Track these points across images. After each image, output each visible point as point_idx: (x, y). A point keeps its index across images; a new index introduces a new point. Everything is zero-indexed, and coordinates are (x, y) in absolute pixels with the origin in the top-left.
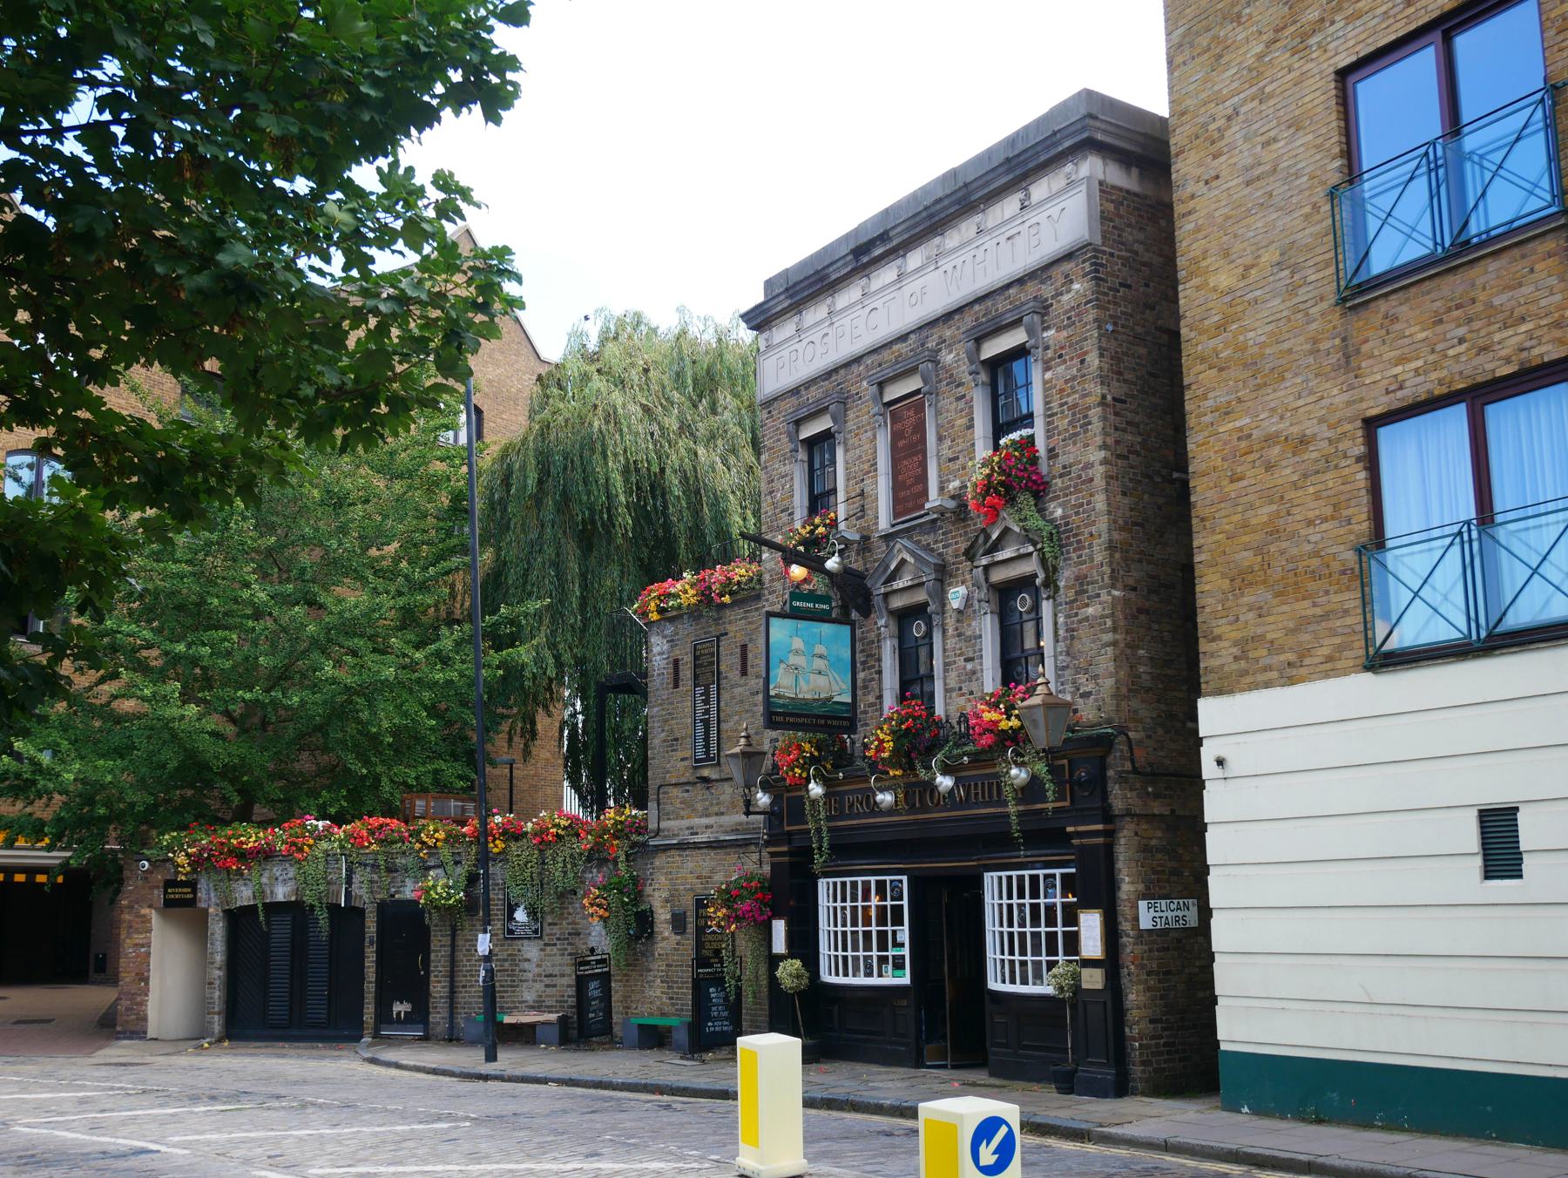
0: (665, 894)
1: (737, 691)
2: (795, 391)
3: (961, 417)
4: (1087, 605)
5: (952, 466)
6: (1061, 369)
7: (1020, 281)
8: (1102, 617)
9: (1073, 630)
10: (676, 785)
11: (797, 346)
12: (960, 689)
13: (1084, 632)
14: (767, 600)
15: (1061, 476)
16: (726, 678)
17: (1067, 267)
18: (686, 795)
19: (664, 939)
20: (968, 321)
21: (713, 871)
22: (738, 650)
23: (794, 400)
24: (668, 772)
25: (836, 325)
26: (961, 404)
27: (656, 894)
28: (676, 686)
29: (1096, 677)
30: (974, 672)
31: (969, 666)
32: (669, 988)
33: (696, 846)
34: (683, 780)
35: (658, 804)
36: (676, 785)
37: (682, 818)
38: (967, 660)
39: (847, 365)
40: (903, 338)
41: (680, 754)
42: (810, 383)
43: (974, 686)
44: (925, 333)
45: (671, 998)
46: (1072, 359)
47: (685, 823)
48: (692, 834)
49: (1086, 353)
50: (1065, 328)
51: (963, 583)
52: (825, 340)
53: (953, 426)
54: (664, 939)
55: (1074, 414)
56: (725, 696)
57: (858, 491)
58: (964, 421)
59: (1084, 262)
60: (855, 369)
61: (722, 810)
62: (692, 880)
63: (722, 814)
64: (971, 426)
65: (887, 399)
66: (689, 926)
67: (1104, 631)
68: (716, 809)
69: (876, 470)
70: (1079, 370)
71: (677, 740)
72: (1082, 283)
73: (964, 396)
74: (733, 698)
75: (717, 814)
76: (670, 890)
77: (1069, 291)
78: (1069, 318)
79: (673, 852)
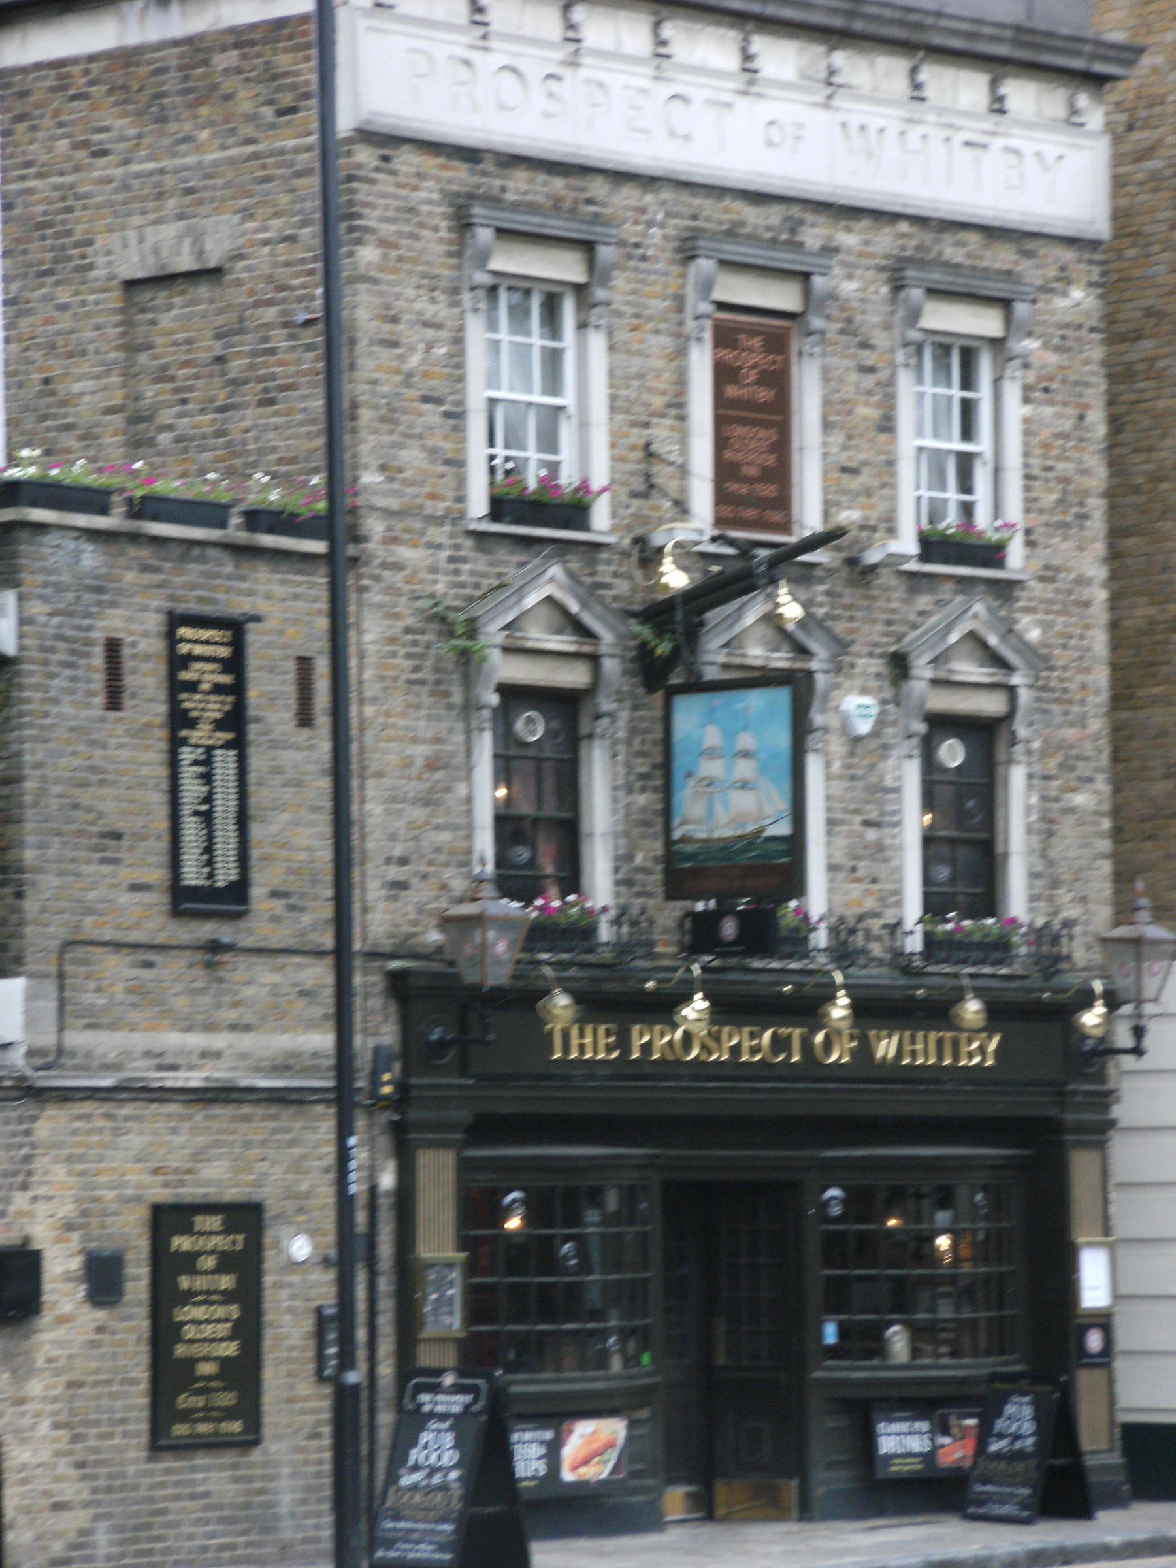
0: (67, 1209)
1: (289, 757)
2: (470, 155)
3: (867, 404)
4: (1074, 790)
5: (853, 483)
6: (1048, 411)
7: (994, 233)
8: (1096, 813)
9: (1052, 821)
10: (117, 946)
11: (476, 57)
12: (854, 869)
13: (1067, 827)
14: (377, 578)
15: (1042, 579)
16: (258, 720)
17: (1068, 255)
18: (147, 974)
19: (62, 1320)
20: (885, 241)
21: (199, 1156)
22: (291, 665)
23: (460, 175)
24: (89, 911)
25: (584, 73)
26: (869, 381)
27: (42, 1209)
28: (114, 699)
29: (1083, 900)
30: (879, 847)
31: (871, 835)
32: (75, 1439)
33: (162, 1095)
34: (135, 936)
35: (62, 988)
36: (117, 946)
37: (133, 1028)
38: (868, 823)
39: (621, 177)
40: (759, 198)
41: (127, 875)
42: (513, 161)
43: (881, 870)
44: (795, 211)
45: (81, 1465)
46: (1065, 404)
47: (139, 1040)
48: (160, 1068)
49: (1087, 407)
50: (1058, 349)
51: (864, 691)
52: (553, 85)
53: (849, 412)
54: (62, 1320)
55: (1064, 492)
56: (257, 761)
57: (642, 441)
58: (874, 413)
59: (1091, 262)
60: (627, 197)
61: (249, 1018)
62: (137, 1176)
63: (247, 1028)
64: (887, 425)
65: (719, 295)
66: (129, 1286)
67: (1100, 835)
68: (232, 1015)
69: (682, 418)
70: (1077, 427)
71: (117, 836)
72: (1088, 296)
73: (871, 370)
74: (277, 770)
75: (233, 1027)
76: (78, 1200)
77: (1065, 294)
78: (1063, 337)
79: (88, 1107)
